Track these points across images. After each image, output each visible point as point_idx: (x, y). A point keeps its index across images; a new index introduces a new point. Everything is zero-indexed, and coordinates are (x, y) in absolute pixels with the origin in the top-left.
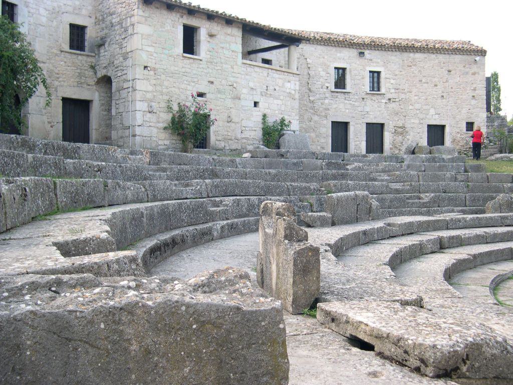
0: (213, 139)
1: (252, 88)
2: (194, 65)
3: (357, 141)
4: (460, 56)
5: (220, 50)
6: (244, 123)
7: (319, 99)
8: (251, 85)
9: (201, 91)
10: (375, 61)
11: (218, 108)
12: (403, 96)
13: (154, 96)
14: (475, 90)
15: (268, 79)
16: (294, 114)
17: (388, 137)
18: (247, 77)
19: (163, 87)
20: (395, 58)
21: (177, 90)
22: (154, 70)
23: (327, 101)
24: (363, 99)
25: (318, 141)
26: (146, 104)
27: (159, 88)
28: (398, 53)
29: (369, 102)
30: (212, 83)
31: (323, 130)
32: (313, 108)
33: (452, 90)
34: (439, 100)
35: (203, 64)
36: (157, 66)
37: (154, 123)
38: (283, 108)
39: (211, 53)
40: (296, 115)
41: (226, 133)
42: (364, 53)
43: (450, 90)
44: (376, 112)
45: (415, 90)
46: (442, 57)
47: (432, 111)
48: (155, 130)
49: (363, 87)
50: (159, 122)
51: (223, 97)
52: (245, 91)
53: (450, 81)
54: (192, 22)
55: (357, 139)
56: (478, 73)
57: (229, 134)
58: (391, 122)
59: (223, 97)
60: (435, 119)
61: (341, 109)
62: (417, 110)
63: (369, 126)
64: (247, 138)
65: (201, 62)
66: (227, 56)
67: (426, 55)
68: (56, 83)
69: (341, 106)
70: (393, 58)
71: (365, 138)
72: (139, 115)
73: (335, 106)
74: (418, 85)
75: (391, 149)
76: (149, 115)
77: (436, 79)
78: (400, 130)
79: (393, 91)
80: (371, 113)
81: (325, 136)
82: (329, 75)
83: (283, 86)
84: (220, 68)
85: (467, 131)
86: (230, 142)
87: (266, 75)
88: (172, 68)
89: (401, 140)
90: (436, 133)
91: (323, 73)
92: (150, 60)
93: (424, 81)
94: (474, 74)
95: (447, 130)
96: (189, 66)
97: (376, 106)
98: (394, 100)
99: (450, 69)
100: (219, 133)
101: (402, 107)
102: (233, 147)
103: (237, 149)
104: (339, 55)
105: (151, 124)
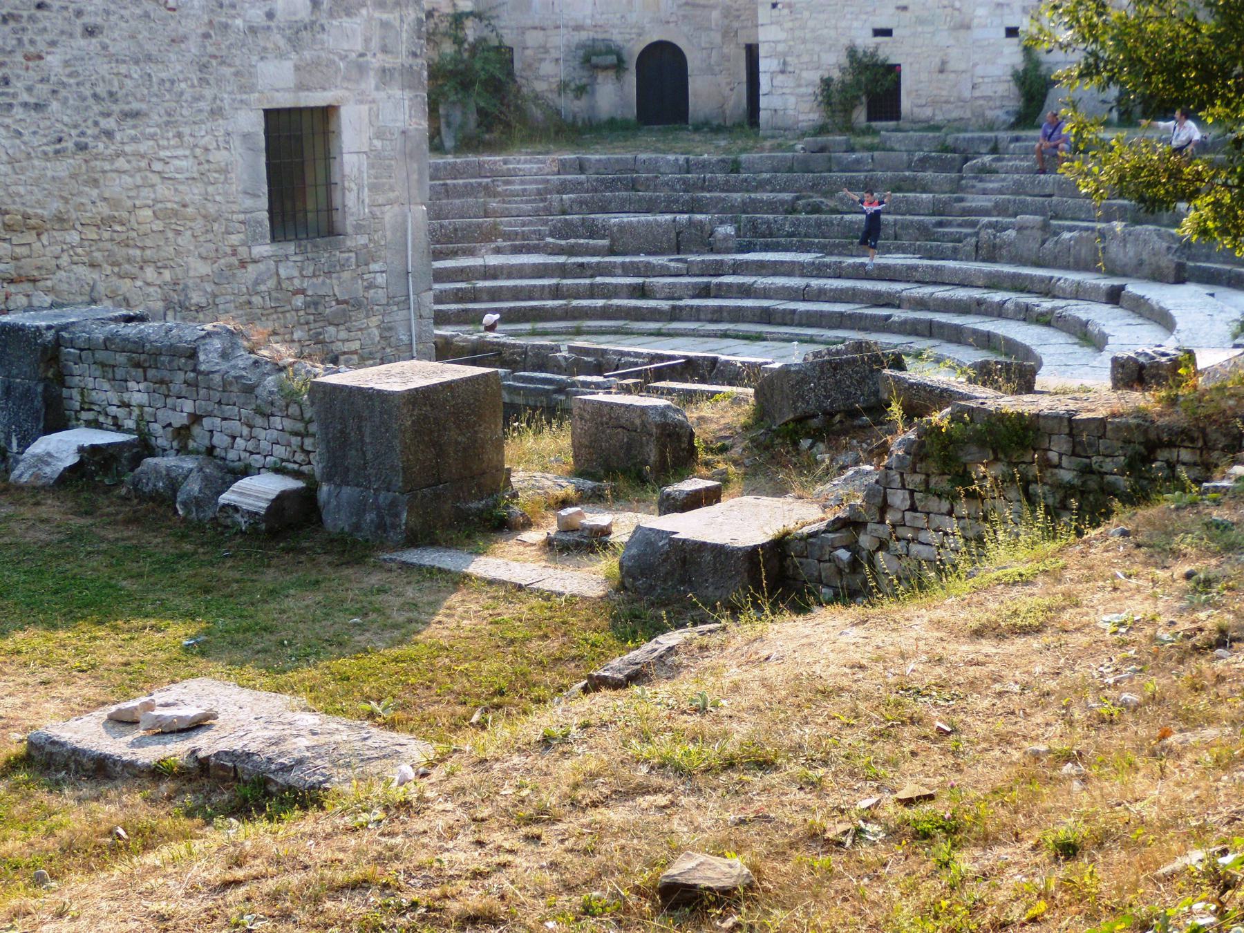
0: (906, 104)
9: (882, 24)
11: (918, 51)
13: (790, 47)
22: (790, 6)
26: (776, 62)
27: (798, 33)
30: (905, 8)
50: (799, 86)
52: (980, 12)
57: (944, 93)
59: (931, 29)
68: (736, 24)
76: (780, 77)
86: (946, 107)
102: (954, 115)
103: (961, 119)
105: (784, 90)
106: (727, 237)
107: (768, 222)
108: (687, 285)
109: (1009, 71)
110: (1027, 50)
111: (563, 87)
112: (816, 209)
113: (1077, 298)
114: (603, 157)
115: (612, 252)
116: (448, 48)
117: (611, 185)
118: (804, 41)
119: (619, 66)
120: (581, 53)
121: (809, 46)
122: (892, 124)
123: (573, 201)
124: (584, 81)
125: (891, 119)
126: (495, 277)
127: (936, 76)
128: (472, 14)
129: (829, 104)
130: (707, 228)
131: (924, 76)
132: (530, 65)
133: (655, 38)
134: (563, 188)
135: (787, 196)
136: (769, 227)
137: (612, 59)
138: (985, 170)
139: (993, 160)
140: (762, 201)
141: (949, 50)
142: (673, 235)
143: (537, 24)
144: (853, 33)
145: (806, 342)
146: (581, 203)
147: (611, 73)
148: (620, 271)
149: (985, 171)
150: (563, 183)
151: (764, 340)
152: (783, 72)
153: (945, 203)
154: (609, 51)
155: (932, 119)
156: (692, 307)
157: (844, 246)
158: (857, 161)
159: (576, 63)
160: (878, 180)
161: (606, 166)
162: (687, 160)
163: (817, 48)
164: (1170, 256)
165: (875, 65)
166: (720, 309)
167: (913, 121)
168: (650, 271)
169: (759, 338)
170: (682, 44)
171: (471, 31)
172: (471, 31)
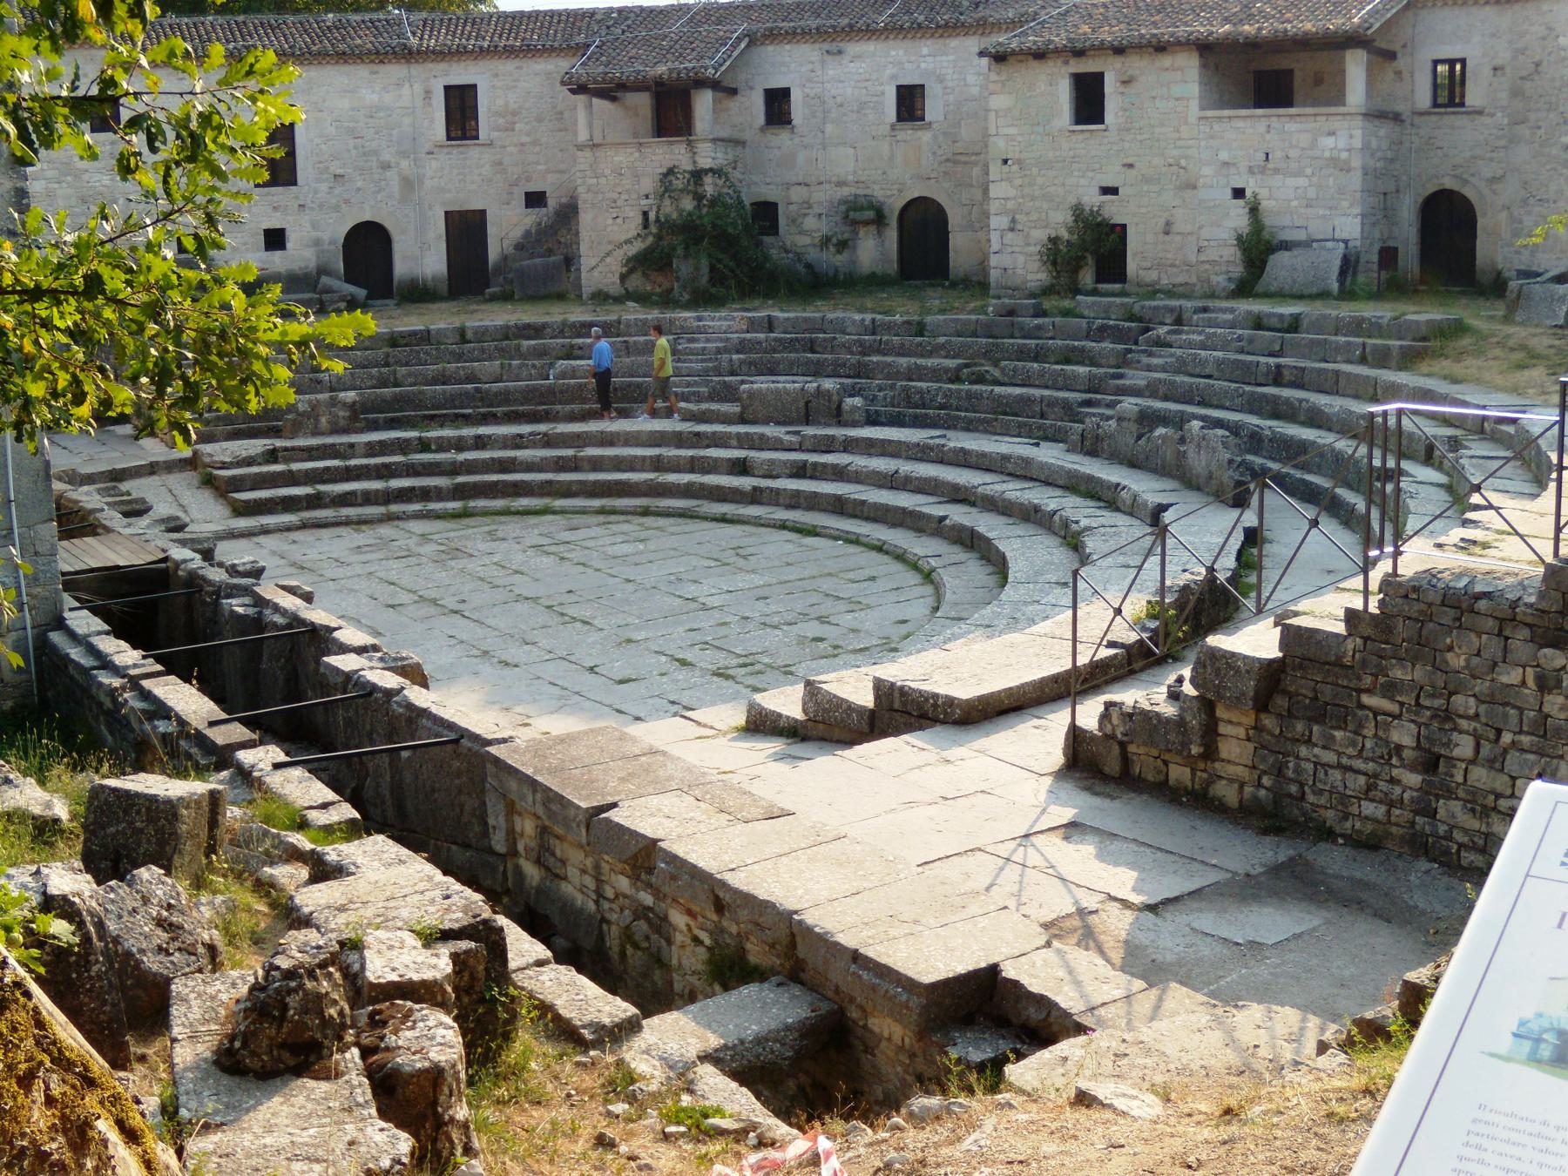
8: (1224, 156)
11: (1143, 210)
15: (1268, 137)
16: (1345, 204)
22: (1019, 162)
27: (1027, 190)
30: (1131, 166)
36: (1024, 155)
38: (1312, 193)
40: (1352, 205)
50: (1028, 245)
52: (1207, 171)
54: (1088, 66)
57: (1169, 256)
64: (1212, 262)
72: (995, 237)
76: (1010, 235)
83: (1313, 144)
88: (1050, 155)
102: (1180, 279)
106: (854, 408)
107: (920, 392)
108: (785, 463)
109: (1233, 235)
110: (1254, 210)
111: (825, 241)
112: (980, 379)
113: (1131, 514)
114: (792, 315)
115: (742, 420)
116: (688, 204)
117: (788, 345)
118: (1033, 199)
119: (879, 219)
120: (843, 208)
121: (1038, 204)
122: (1117, 286)
123: (742, 362)
124: (846, 236)
125: (1115, 282)
126: (611, 444)
127: (1162, 237)
128: (711, 170)
129: (1054, 263)
130: (835, 398)
131: (1150, 238)
132: (794, 221)
133: (916, 195)
134: (741, 347)
135: (951, 363)
136: (922, 398)
137: (871, 214)
138: (1161, 343)
139: (1169, 332)
140: (926, 368)
142: (802, 404)
143: (801, 180)
144: (1080, 190)
145: (851, 542)
146: (750, 363)
147: (873, 229)
148: (734, 443)
149: (1161, 343)
150: (742, 341)
151: (817, 535)
152: (1012, 230)
153: (1101, 380)
154: (871, 206)
155: (1157, 282)
156: (771, 489)
157: (988, 422)
158: (1039, 327)
159: (838, 218)
160: (1049, 349)
161: (794, 325)
162: (873, 320)
163: (1045, 206)
164: (1231, 472)
165: (1099, 225)
166: (797, 494)
167: (1138, 285)
168: (763, 443)
169: (812, 532)
170: (942, 199)
171: (710, 187)
172: (710, 187)
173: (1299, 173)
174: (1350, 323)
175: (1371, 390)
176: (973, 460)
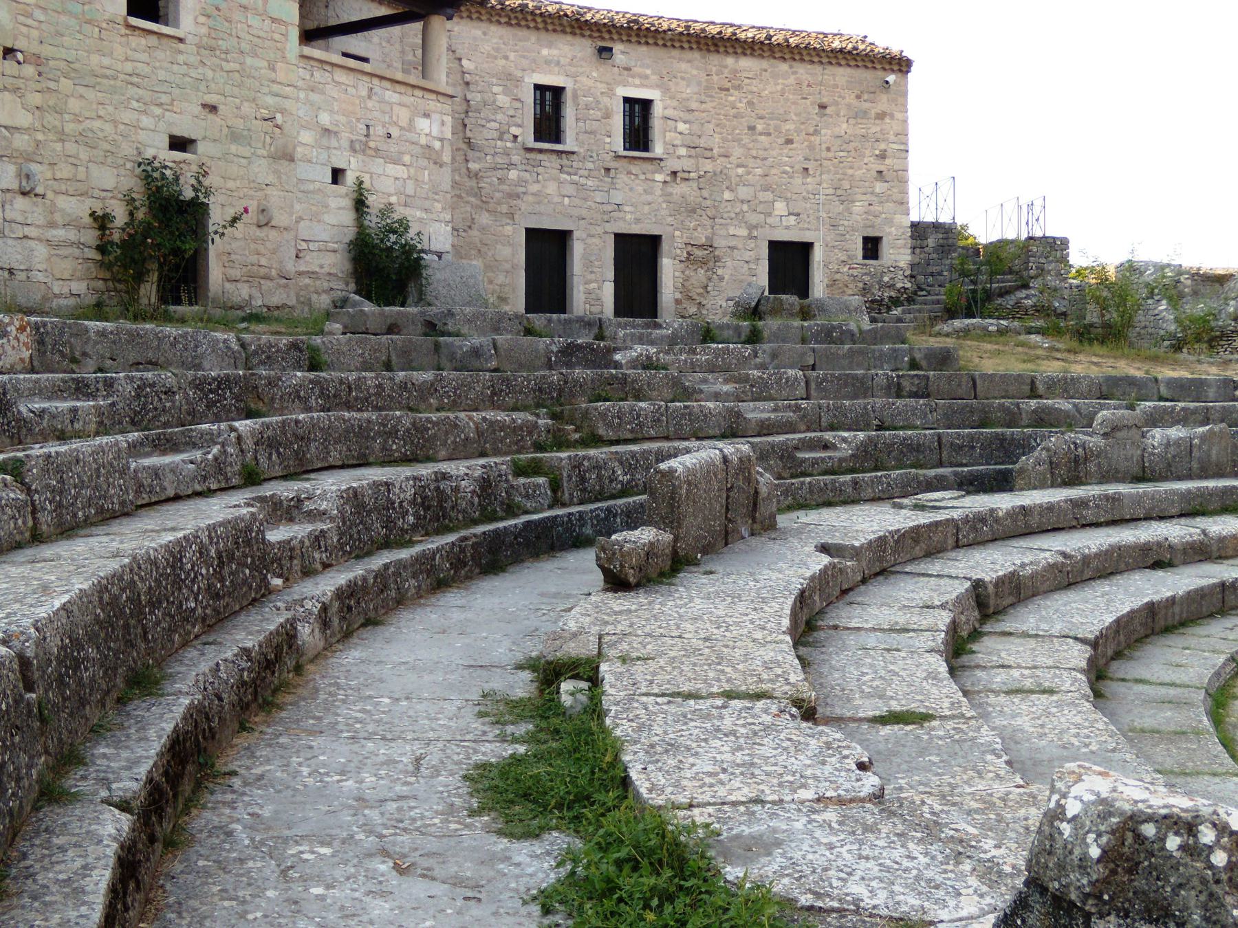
0: (216, 273)
1: (327, 130)
2: (160, 54)
3: (593, 283)
4: (849, 70)
5: (237, 15)
6: (305, 230)
7: (495, 169)
8: (325, 119)
9: (182, 131)
10: (639, 73)
11: (231, 184)
12: (708, 166)
13: (38, 144)
14: (883, 156)
15: (370, 104)
16: (438, 206)
17: (670, 273)
18: (314, 97)
19: (67, 117)
20: (690, 68)
21: (108, 128)
22: (38, 60)
23: (513, 174)
24: (608, 170)
25: (491, 282)
26: (11, 169)
28: (696, 55)
29: (622, 178)
30: (213, 109)
31: (504, 252)
32: (478, 193)
33: (830, 155)
34: (798, 180)
35: (189, 53)
36: (46, 50)
37: (38, 226)
38: (410, 189)
39: (211, 22)
40: (444, 209)
41: (254, 259)
42: (611, 49)
43: (825, 154)
44: (640, 202)
45: (737, 152)
46: (804, 72)
47: (780, 207)
48: (41, 251)
49: (608, 140)
50: (52, 225)
51: (246, 151)
52: (306, 137)
53: (823, 132)
55: (593, 277)
56: (892, 116)
57: (263, 262)
58: (677, 233)
59: (246, 151)
60: (787, 228)
61: (551, 196)
62: (742, 202)
63: (622, 240)
64: (312, 274)
65: (181, 46)
66: (255, 32)
67: (765, 64)
69: (551, 188)
70: (684, 66)
71: (611, 275)
73: (535, 188)
74: (746, 140)
75: (678, 302)
76: (20, 202)
77: (789, 126)
78: (699, 253)
79: (683, 151)
80: (627, 209)
81: (507, 266)
82: (518, 105)
83: (411, 127)
84: (237, 67)
85: (865, 257)
86: (267, 284)
87: (364, 93)
89: (704, 280)
90: (789, 262)
91: (503, 100)
92: (24, 30)
93: (759, 128)
94: (881, 116)
95: (818, 255)
96: (144, 57)
97: (640, 189)
98: (686, 175)
99: (825, 100)
100: (233, 257)
101: (705, 193)
102: (275, 300)
103: (284, 306)
104: (545, 52)
105: (27, 231)
118: (62, 137)
141: (269, 191)
144: (142, 136)
155: (248, 302)
163: (84, 154)
173: (397, 162)
174: (818, 332)
175: (1027, 388)
176: (1034, 521)
